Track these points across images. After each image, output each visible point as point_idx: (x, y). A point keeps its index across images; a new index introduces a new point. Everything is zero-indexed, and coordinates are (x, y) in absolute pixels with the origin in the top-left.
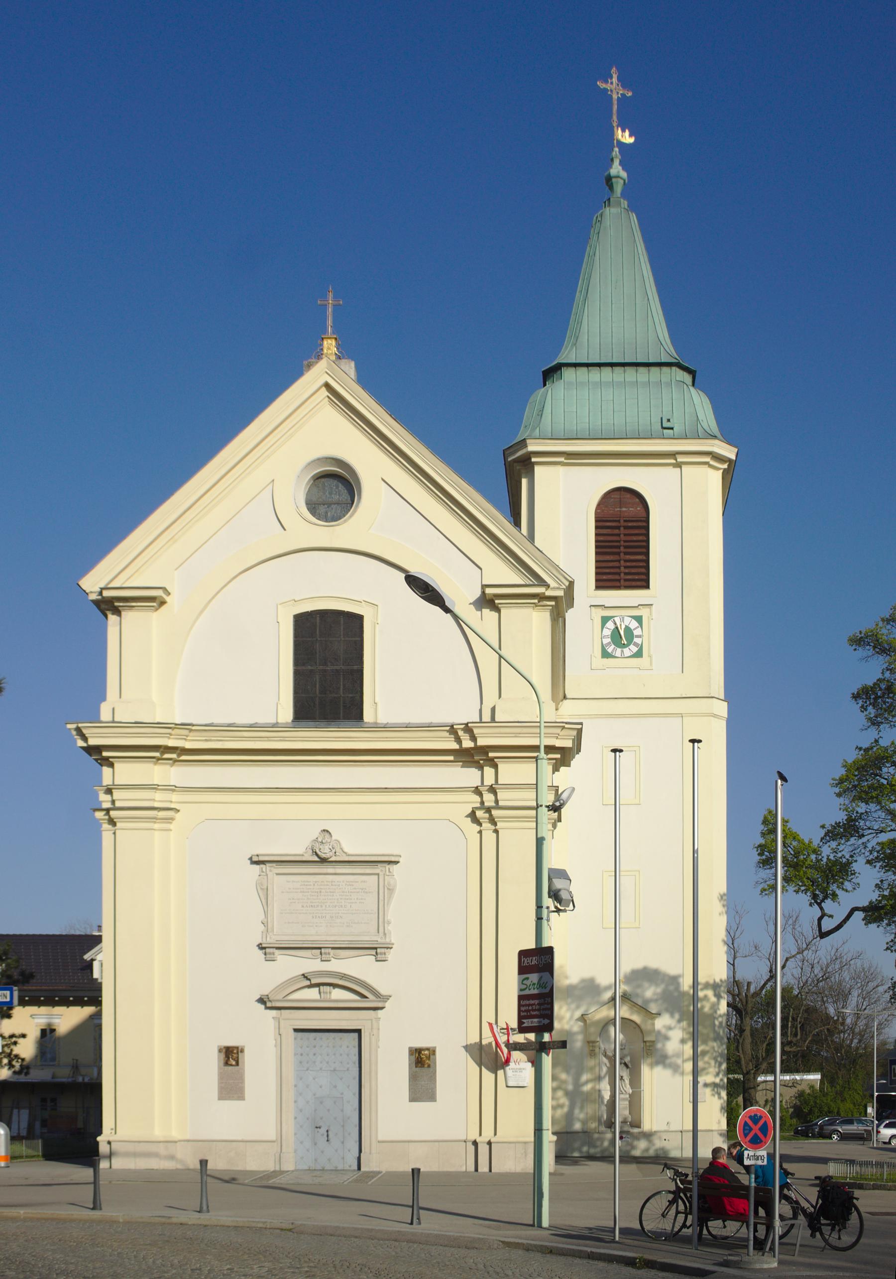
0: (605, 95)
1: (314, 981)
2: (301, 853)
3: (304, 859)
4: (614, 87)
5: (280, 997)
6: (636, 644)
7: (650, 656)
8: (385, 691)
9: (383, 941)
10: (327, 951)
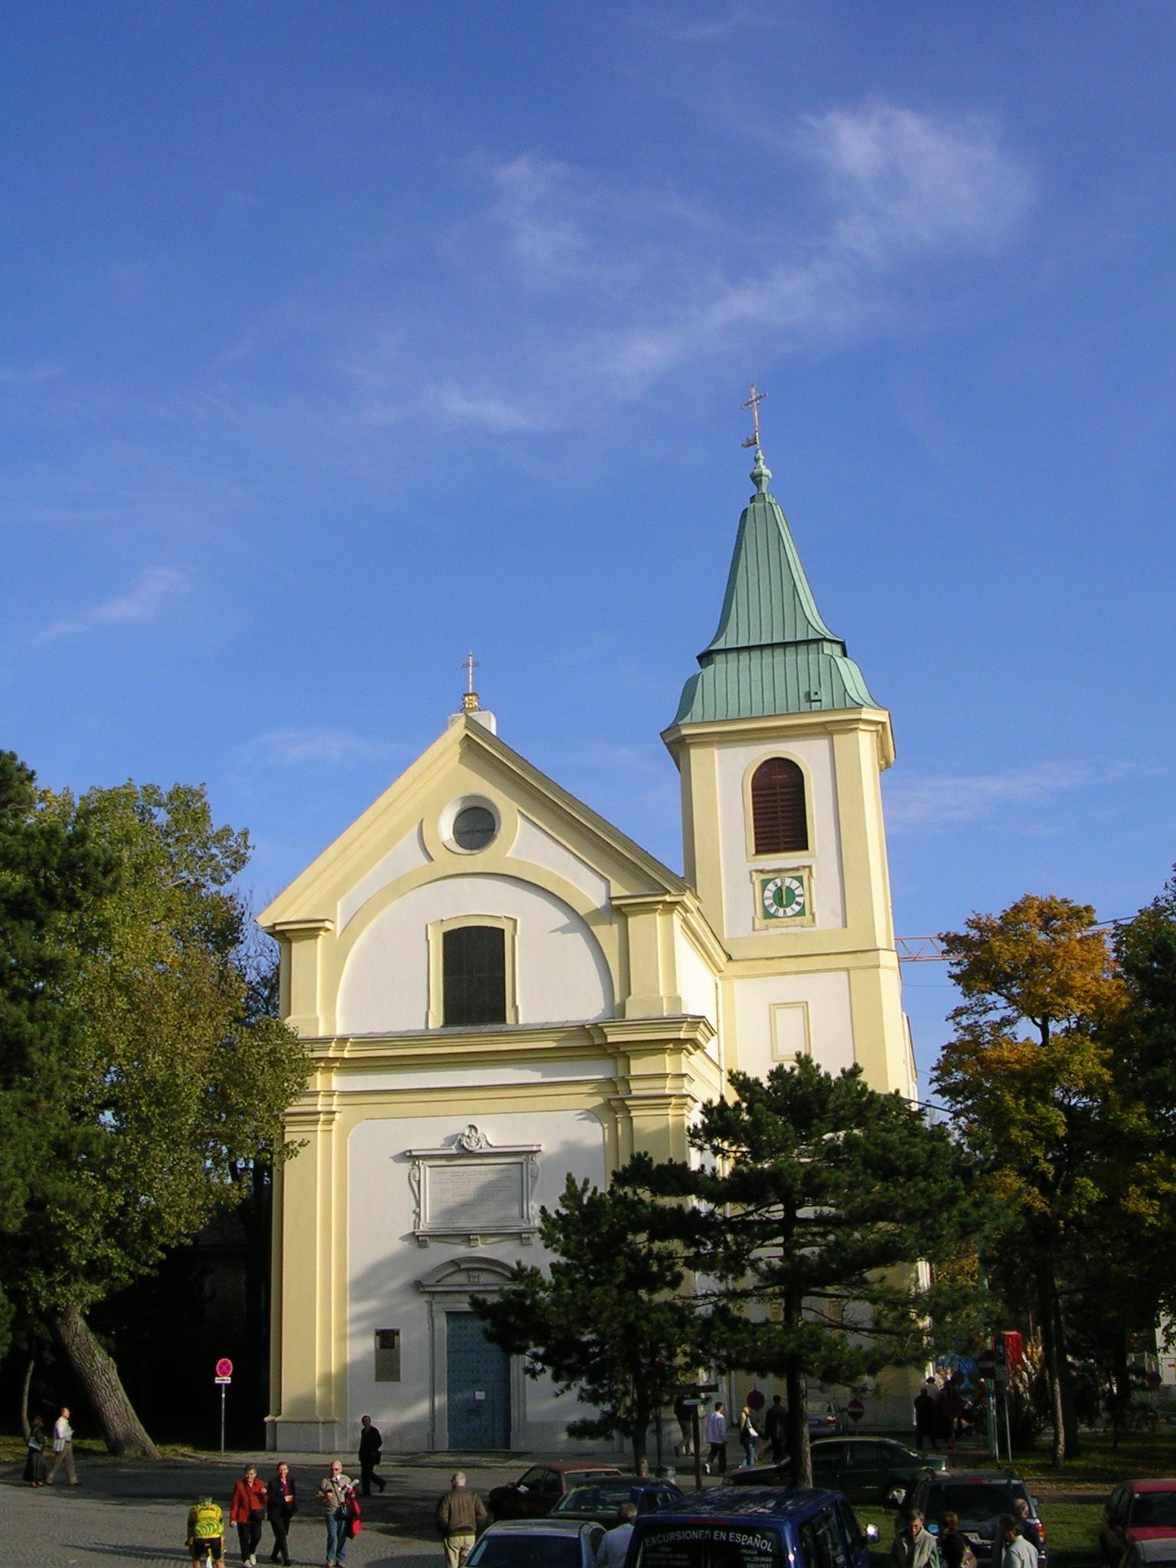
6: (798, 904)
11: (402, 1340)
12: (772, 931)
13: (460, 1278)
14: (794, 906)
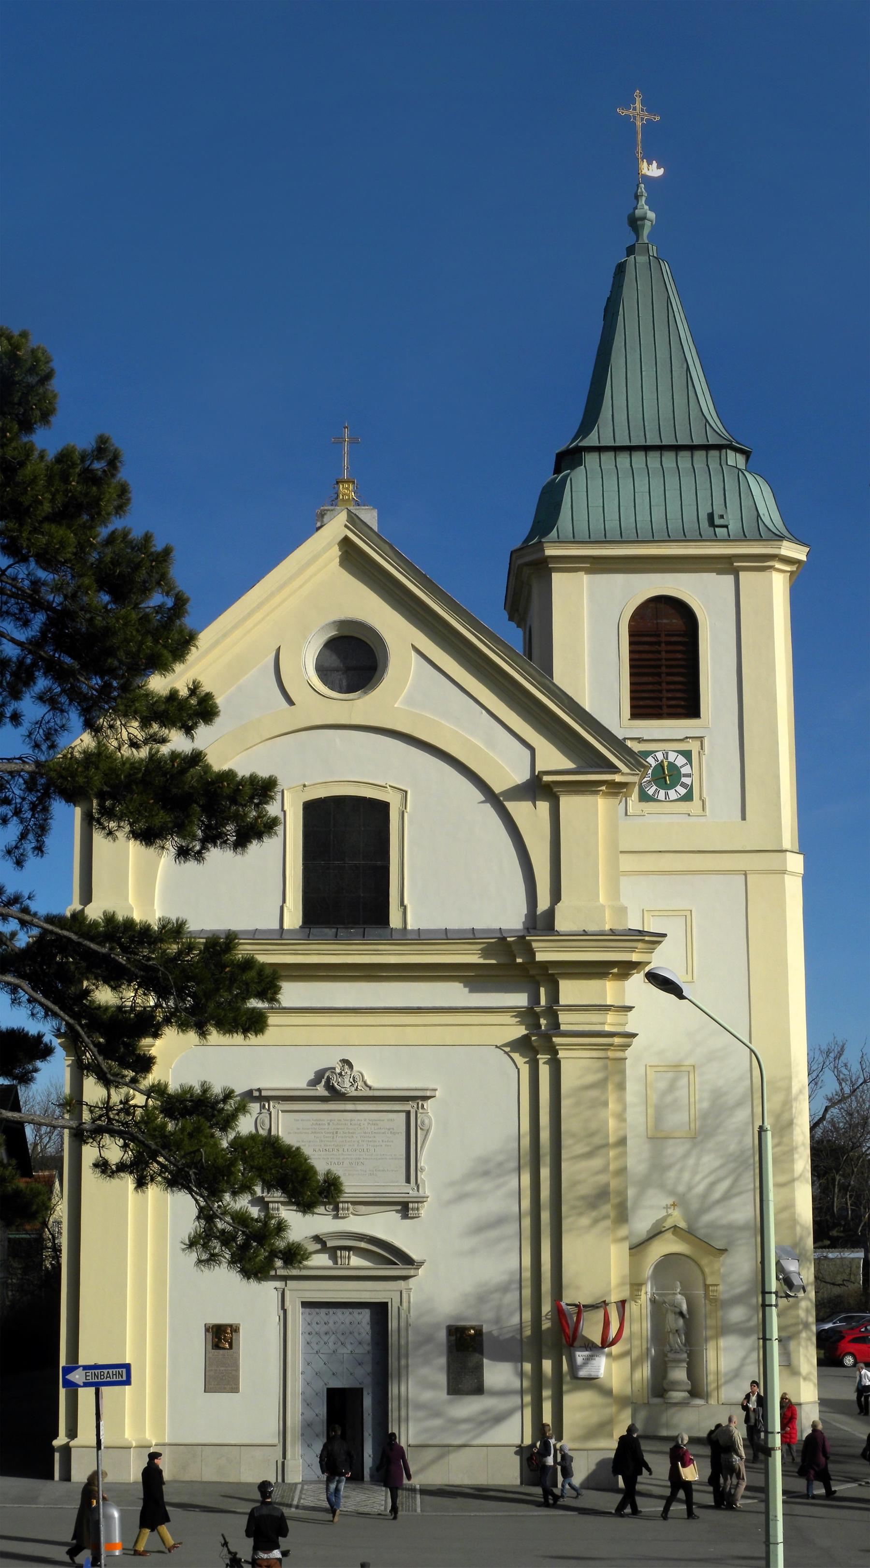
0: (628, 123)
4: (638, 112)
9: (415, 1193)
11: (244, 1340)
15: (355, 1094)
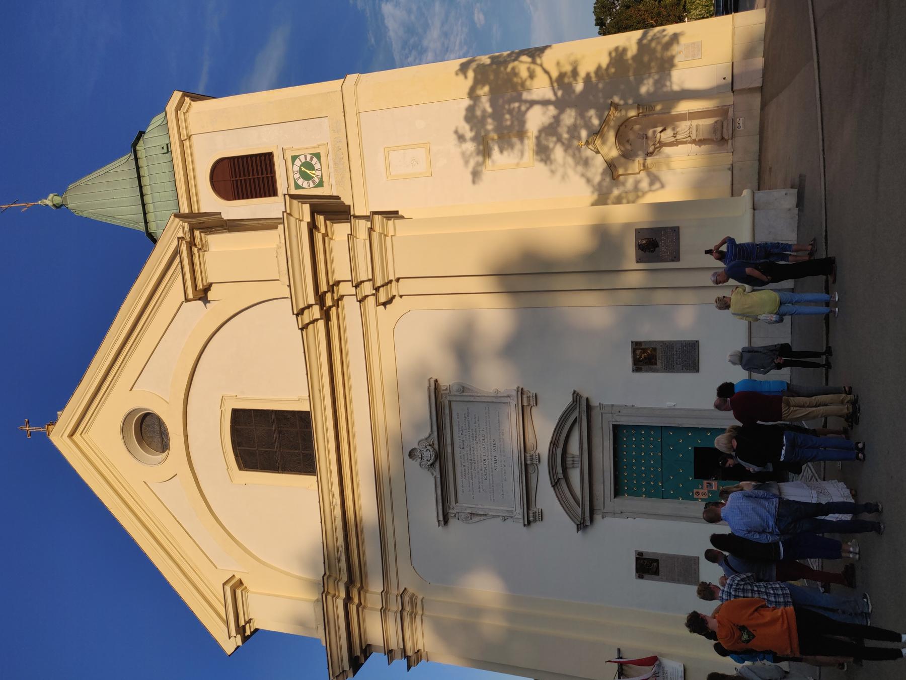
1: (561, 476)
2: (433, 479)
3: (438, 476)
5: (579, 511)
6: (311, 159)
7: (318, 147)
8: (285, 393)
10: (528, 458)
11: (652, 548)
12: (333, 181)
13: (575, 476)
14: (313, 163)
15: (436, 447)
